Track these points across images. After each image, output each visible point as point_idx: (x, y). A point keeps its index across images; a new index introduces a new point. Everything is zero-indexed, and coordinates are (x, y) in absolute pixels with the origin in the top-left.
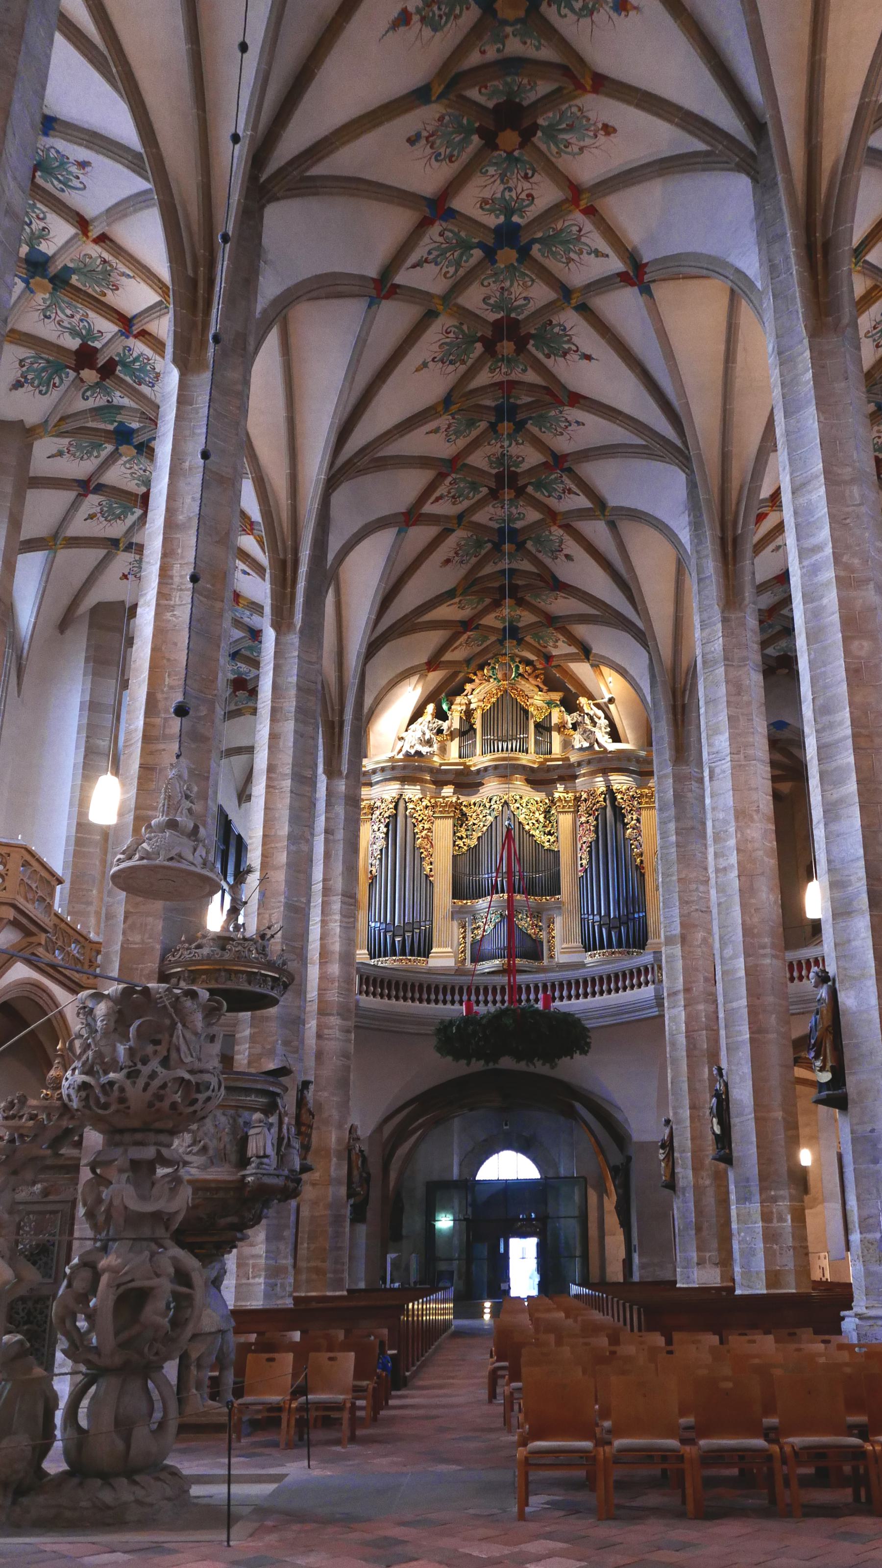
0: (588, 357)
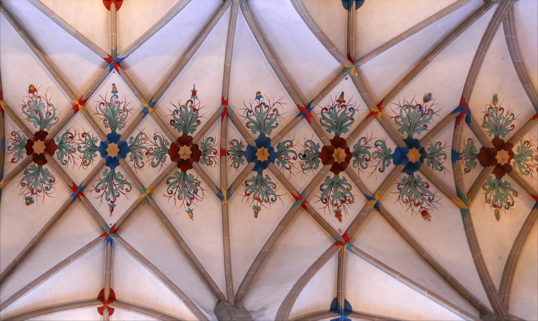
0: (194, 93)
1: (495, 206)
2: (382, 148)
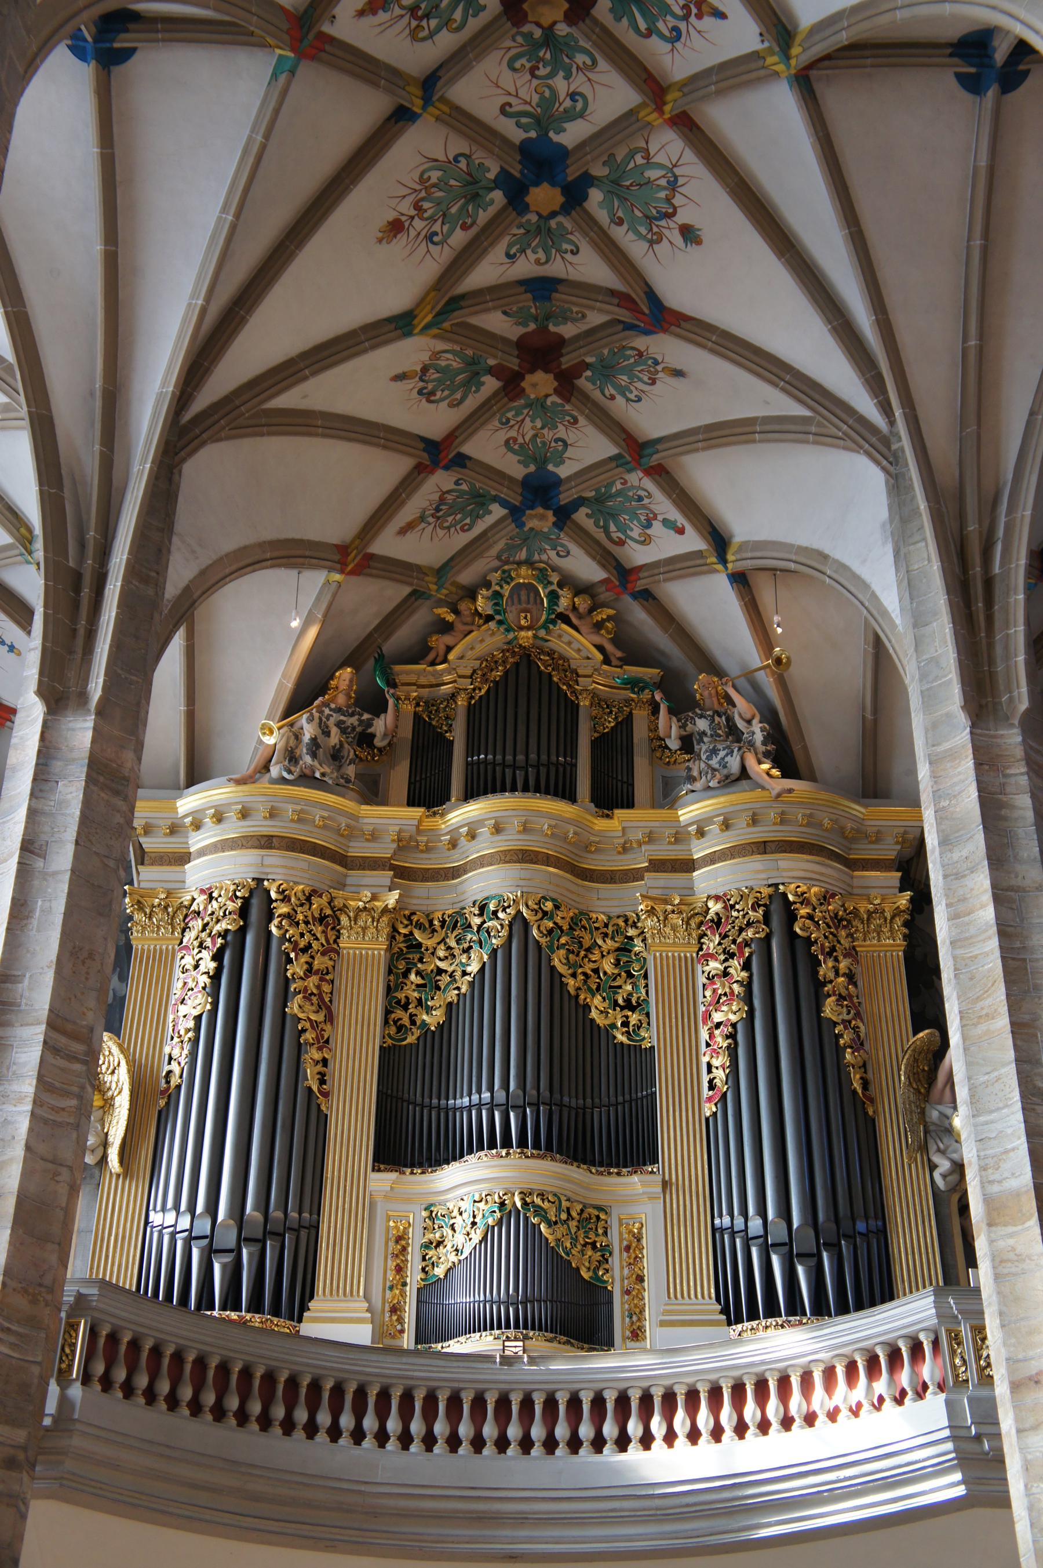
1: (425, 369)
2: (565, 111)
